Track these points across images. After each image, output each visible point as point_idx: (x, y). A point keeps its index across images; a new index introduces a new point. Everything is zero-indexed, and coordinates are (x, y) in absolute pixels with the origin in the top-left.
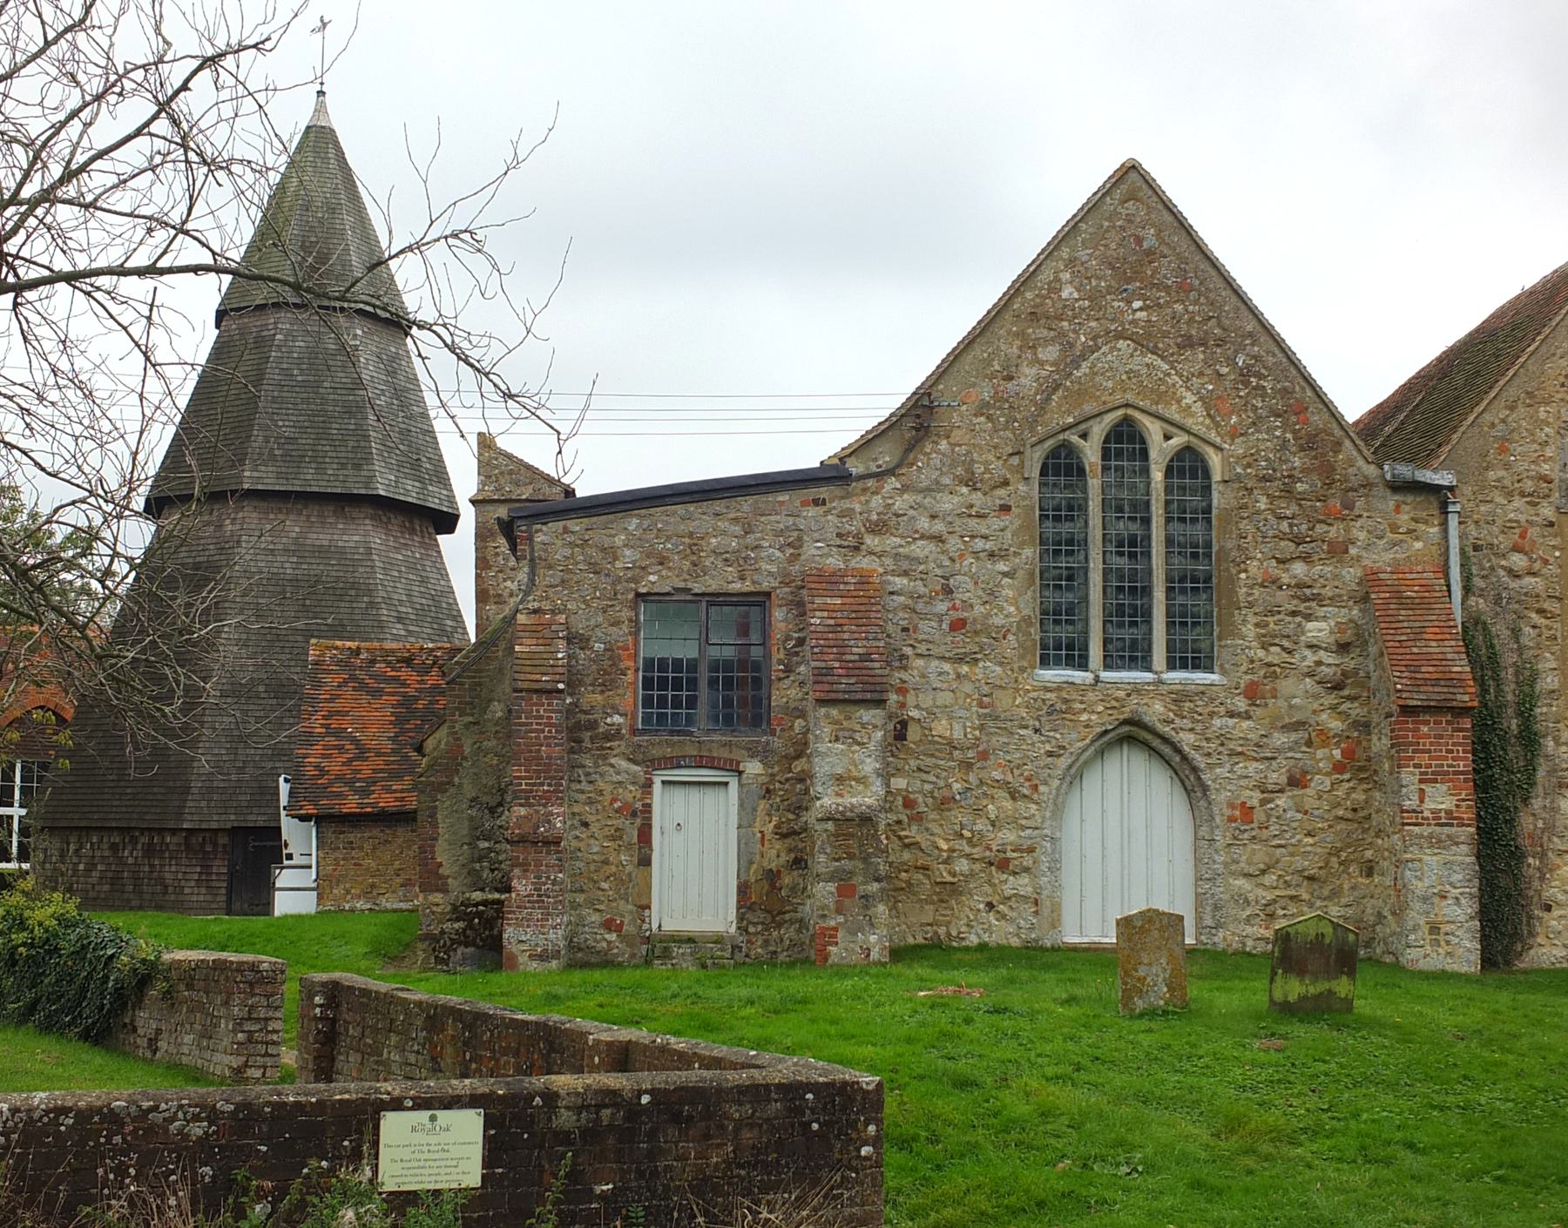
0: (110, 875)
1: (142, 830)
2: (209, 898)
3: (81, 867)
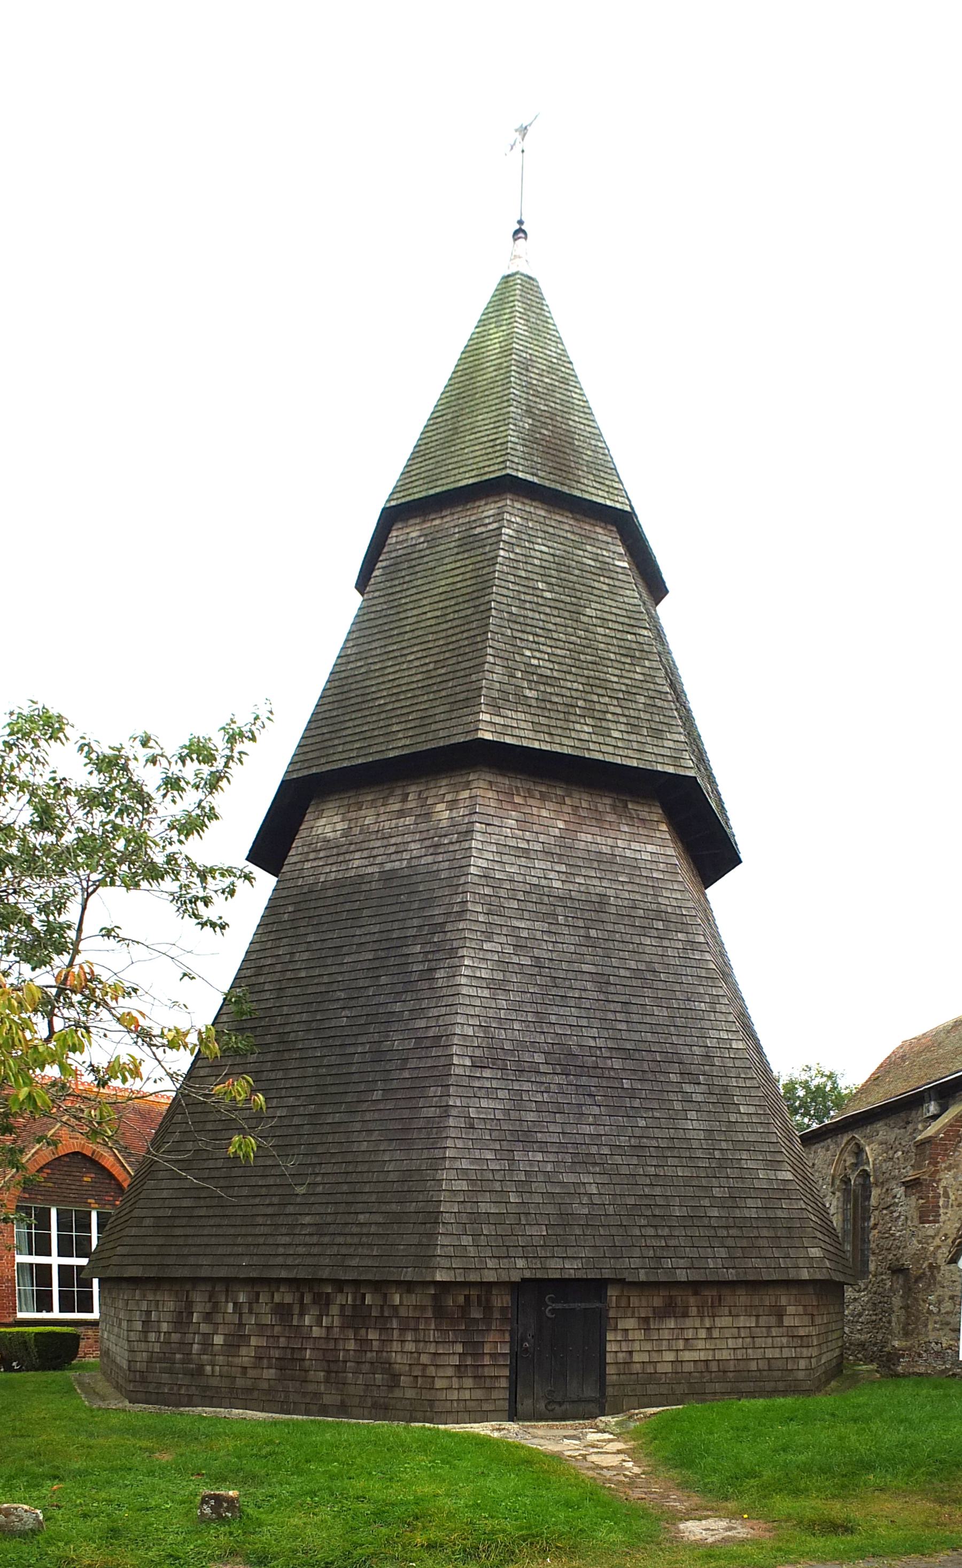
0: (276, 1353)
1: (339, 1285)
2: (478, 1394)
3: (218, 1340)
